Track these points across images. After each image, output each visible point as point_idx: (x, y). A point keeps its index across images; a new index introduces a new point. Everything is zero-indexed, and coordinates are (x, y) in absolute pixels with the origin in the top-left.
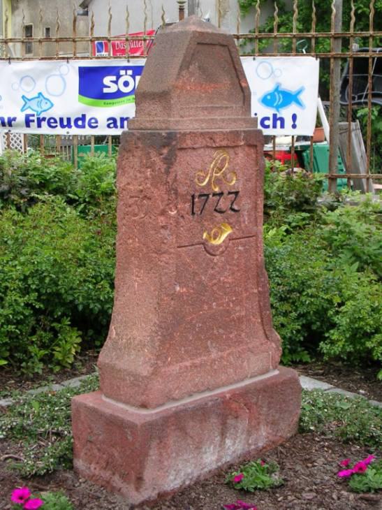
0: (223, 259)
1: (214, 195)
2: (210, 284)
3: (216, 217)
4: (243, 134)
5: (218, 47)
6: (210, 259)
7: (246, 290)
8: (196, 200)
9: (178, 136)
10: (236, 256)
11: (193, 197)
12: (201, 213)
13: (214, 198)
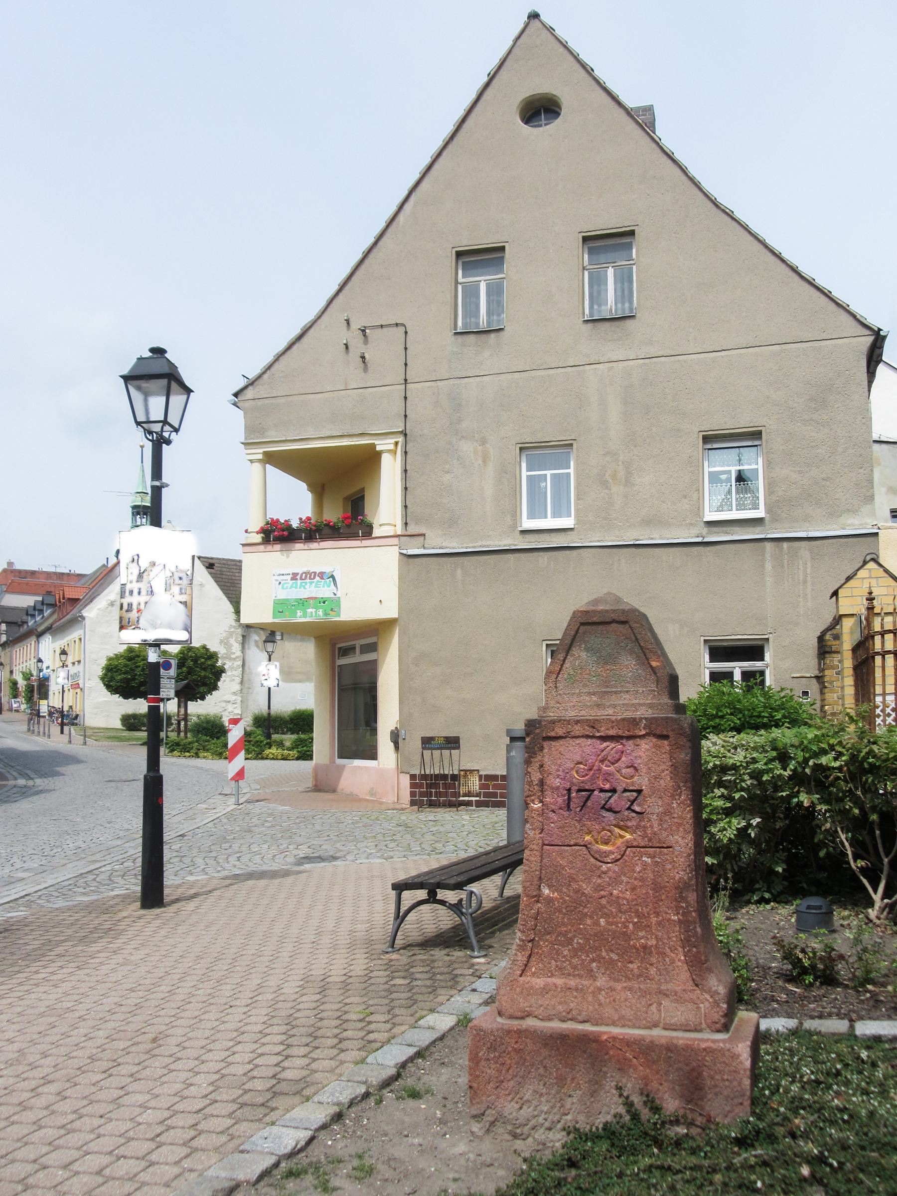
0: (616, 869)
1: (602, 790)
2: (596, 895)
3: (604, 817)
4: (644, 722)
5: (614, 625)
6: (595, 866)
7: (657, 914)
8: (574, 795)
9: (543, 723)
10: (638, 869)
11: (569, 790)
12: (581, 810)
13: (602, 795)
